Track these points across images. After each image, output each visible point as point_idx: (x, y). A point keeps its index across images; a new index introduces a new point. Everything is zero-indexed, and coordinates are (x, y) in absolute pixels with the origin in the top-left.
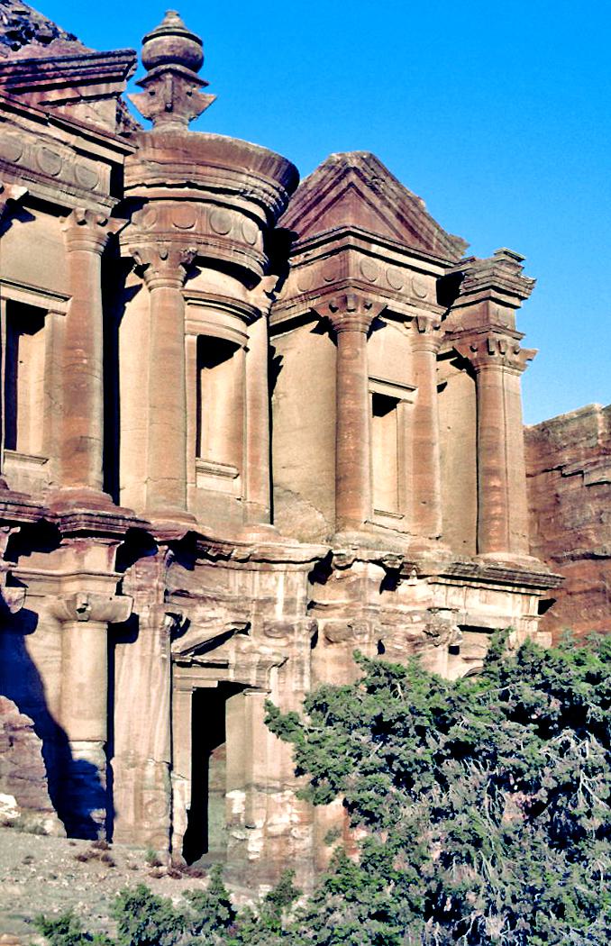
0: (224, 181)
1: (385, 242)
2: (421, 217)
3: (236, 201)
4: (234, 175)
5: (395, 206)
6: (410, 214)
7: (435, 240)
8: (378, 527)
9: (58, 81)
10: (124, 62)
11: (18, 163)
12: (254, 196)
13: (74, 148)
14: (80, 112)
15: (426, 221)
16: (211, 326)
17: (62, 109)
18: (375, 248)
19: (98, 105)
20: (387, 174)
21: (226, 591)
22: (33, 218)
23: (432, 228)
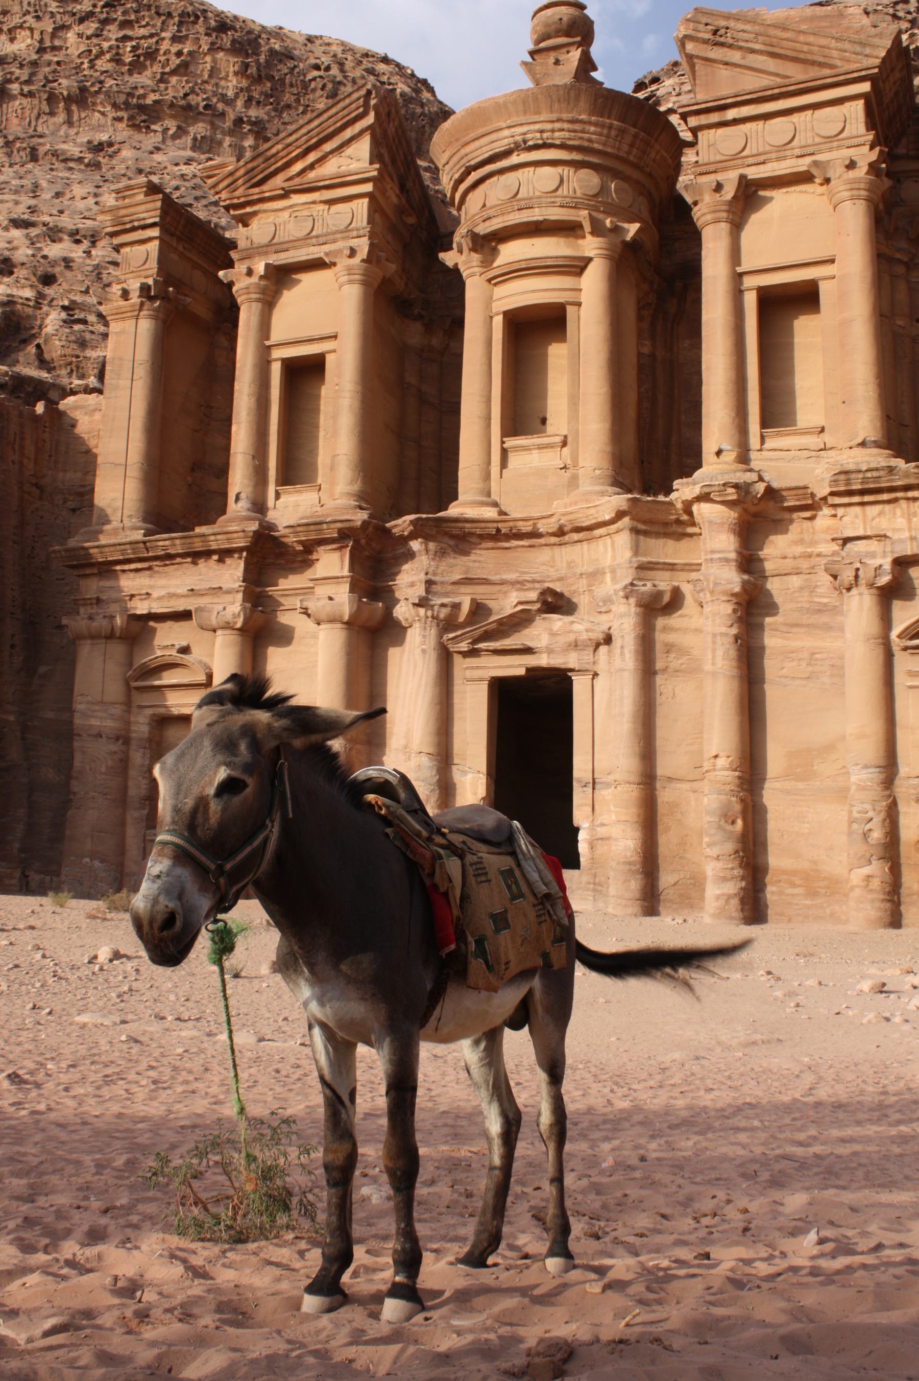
0: (488, 148)
1: (739, 99)
2: (802, 38)
3: (515, 159)
4: (494, 137)
5: (757, 47)
6: (785, 43)
7: (835, 53)
8: (771, 453)
9: (294, 154)
10: (359, 99)
11: (275, 241)
12: (530, 143)
13: (321, 202)
14: (331, 168)
15: (811, 39)
16: (514, 298)
17: (312, 175)
18: (731, 114)
19: (349, 151)
20: (728, 17)
21: (552, 570)
22: (299, 281)
23: (823, 42)
